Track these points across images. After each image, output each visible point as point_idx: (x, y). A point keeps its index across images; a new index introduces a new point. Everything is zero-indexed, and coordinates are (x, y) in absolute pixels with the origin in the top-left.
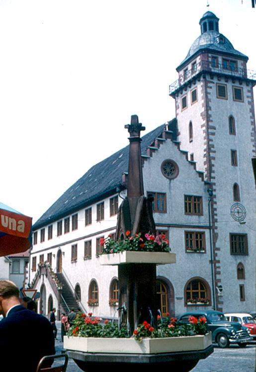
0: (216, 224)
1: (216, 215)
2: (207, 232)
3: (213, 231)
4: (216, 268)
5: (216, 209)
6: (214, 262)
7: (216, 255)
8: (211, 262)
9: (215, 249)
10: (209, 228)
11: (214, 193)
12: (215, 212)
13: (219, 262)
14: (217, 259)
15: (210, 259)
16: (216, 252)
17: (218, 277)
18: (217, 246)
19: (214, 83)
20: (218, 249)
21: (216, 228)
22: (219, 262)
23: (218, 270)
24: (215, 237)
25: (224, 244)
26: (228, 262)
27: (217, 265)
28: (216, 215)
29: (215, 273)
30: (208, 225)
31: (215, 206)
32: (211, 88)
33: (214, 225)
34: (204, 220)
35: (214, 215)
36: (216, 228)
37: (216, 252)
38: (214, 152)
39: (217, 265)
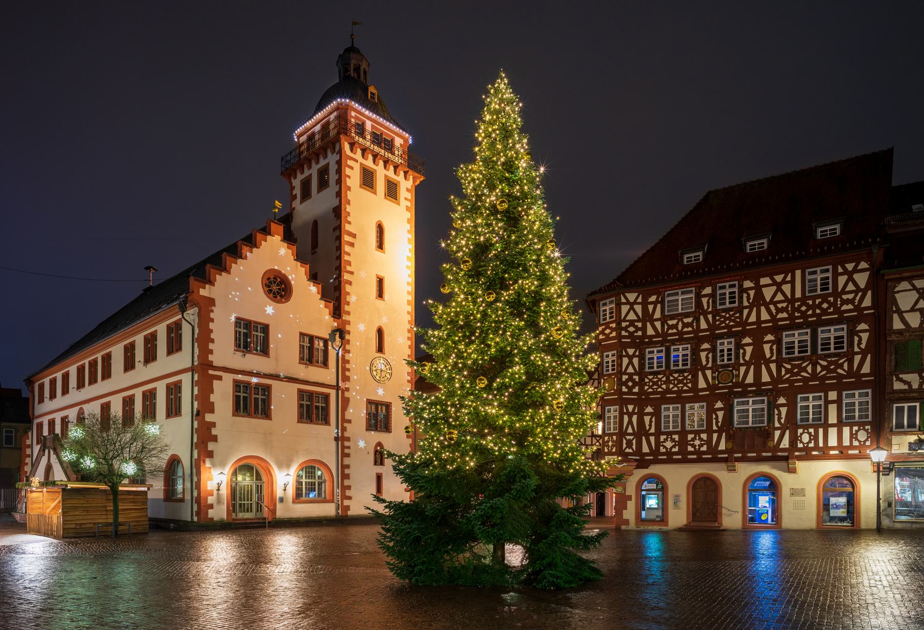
1: (349, 370)
2: (333, 393)
4: (343, 447)
5: (348, 362)
6: (341, 440)
7: (344, 429)
8: (336, 439)
9: (343, 421)
10: (337, 388)
11: (347, 337)
12: (347, 366)
13: (348, 439)
14: (346, 434)
16: (345, 425)
17: (347, 461)
18: (347, 417)
19: (356, 161)
20: (349, 421)
22: (348, 439)
23: (346, 451)
24: (346, 401)
25: (358, 413)
27: (346, 444)
31: (347, 357)
32: (352, 168)
34: (327, 375)
35: (345, 369)
37: (345, 425)
38: (352, 273)
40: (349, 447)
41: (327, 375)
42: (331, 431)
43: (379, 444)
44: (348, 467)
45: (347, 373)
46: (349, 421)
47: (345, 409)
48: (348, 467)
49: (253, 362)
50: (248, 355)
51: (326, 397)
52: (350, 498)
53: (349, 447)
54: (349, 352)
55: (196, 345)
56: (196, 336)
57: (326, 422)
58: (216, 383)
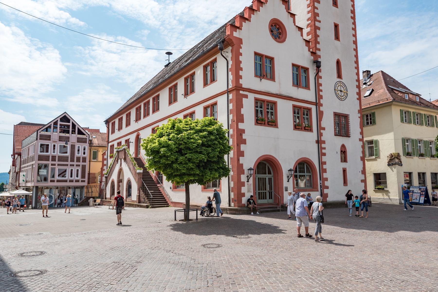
0: (322, 101)
2: (313, 108)
3: (319, 108)
7: (321, 135)
8: (318, 142)
9: (320, 128)
12: (321, 88)
13: (324, 142)
15: (317, 139)
16: (322, 131)
20: (324, 129)
21: (322, 105)
23: (324, 151)
24: (320, 115)
25: (328, 122)
26: (333, 143)
27: (323, 146)
28: (321, 91)
29: (321, 154)
30: (315, 101)
33: (319, 101)
34: (309, 95)
36: (322, 105)
37: (322, 131)
38: (320, 22)
39: (323, 146)
40: (325, 148)
41: (309, 95)
42: (313, 136)
43: (343, 146)
44: (325, 163)
45: (321, 93)
46: (324, 129)
47: (321, 120)
48: (325, 163)
49: (265, 85)
50: (263, 80)
51: (310, 110)
52: (327, 188)
53: (325, 148)
54: (321, 77)
55: (230, 73)
56: (230, 67)
57: (311, 130)
58: (244, 99)
